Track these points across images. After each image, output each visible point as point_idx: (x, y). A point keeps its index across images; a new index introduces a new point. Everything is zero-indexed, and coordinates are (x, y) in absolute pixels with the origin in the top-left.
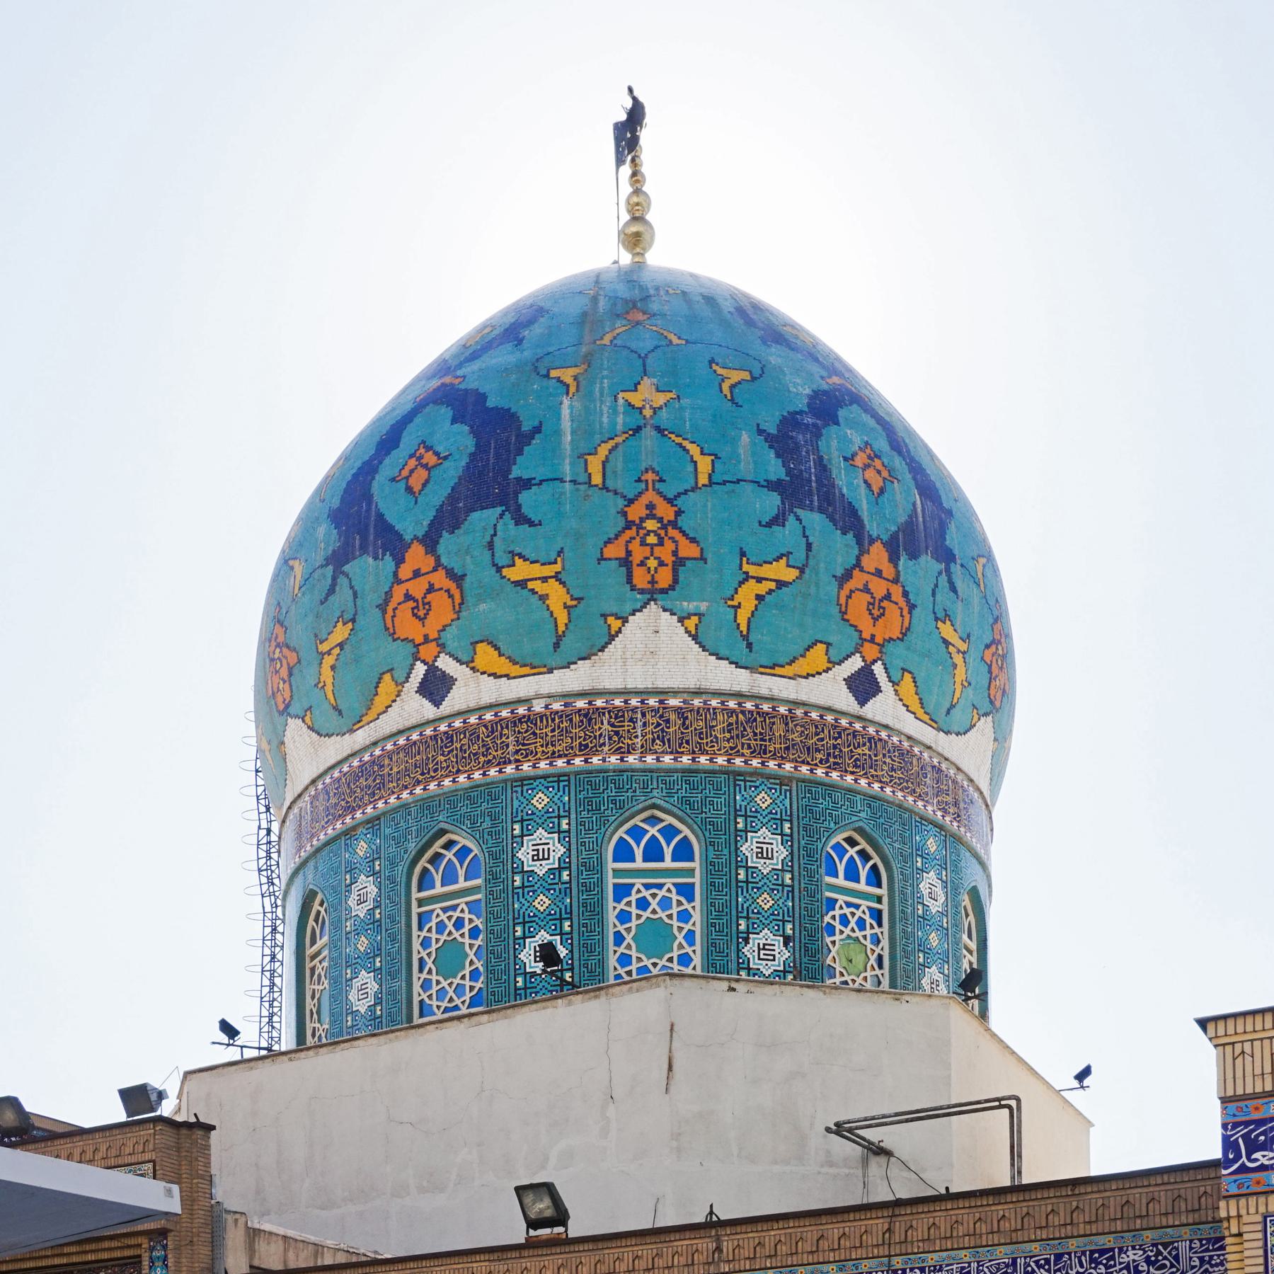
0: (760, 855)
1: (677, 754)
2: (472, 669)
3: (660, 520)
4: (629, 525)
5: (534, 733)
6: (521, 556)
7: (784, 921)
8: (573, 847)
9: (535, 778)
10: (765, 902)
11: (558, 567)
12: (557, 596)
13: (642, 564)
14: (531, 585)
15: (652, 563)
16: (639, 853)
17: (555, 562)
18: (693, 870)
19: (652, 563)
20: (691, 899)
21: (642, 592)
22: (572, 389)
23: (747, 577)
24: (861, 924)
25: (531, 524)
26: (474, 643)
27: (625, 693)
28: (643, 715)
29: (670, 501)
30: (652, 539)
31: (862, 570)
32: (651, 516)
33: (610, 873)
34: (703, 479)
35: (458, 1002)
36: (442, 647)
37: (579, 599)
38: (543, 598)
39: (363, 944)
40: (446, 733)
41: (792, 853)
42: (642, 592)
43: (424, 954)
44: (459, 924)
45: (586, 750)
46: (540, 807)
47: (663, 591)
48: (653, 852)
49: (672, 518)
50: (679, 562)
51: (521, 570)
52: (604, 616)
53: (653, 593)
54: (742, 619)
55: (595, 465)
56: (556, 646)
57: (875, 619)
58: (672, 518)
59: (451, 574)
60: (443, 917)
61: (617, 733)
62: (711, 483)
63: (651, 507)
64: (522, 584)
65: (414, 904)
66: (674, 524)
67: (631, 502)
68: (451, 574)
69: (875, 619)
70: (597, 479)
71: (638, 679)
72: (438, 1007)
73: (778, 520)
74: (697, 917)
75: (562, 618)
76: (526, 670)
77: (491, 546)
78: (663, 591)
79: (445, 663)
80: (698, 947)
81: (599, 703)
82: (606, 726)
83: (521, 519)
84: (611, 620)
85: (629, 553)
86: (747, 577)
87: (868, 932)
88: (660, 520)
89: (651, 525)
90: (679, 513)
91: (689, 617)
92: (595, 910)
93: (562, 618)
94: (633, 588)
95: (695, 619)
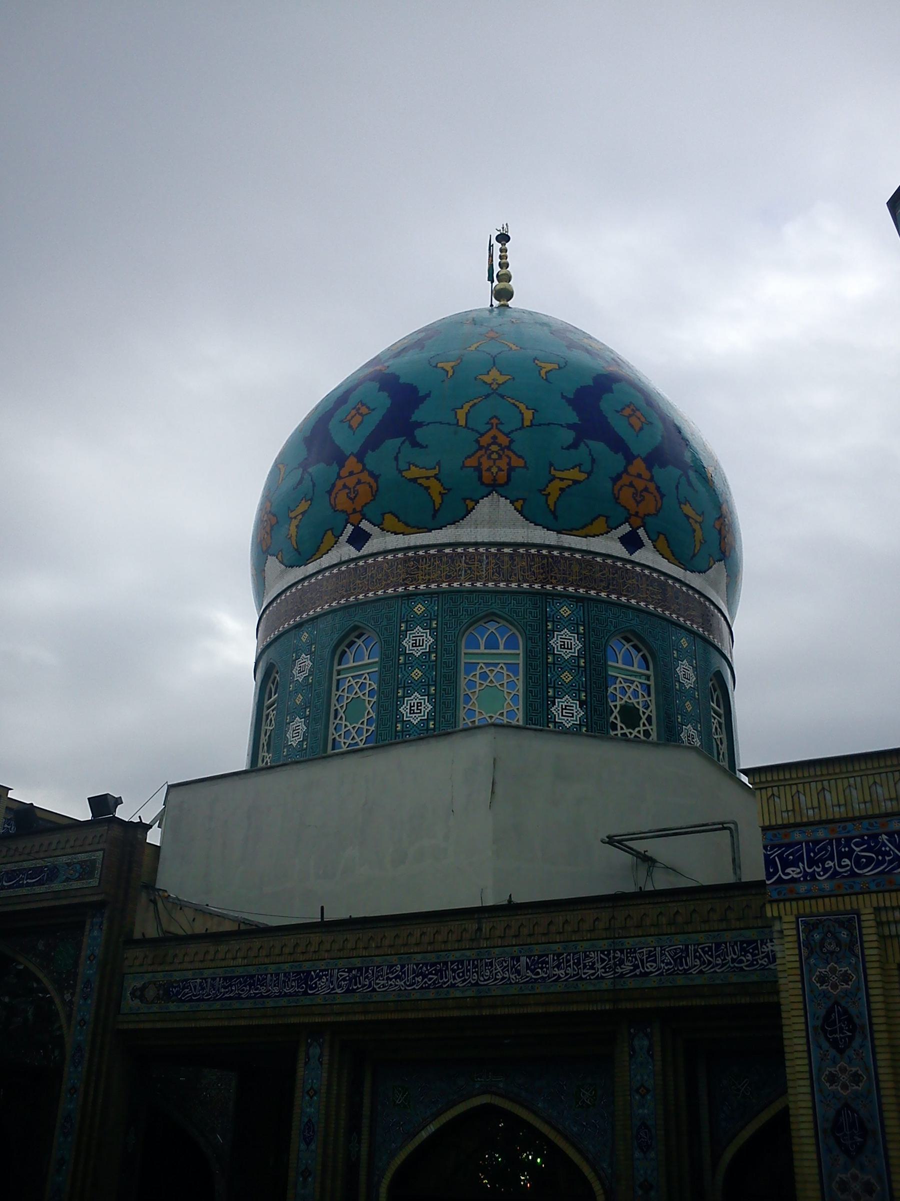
0: (563, 646)
1: (509, 582)
2: (383, 530)
3: (500, 445)
4: (481, 448)
5: (418, 568)
6: (414, 465)
7: (579, 690)
8: (439, 638)
9: (417, 595)
10: (567, 677)
11: (436, 471)
12: (436, 488)
13: (489, 469)
14: (419, 481)
15: (494, 470)
16: (482, 643)
17: (435, 468)
18: (519, 654)
19: (494, 470)
20: (516, 674)
21: (487, 485)
22: (450, 374)
23: (554, 478)
24: (635, 694)
25: (421, 446)
26: (383, 514)
27: (476, 545)
28: (487, 558)
29: (507, 435)
30: (495, 456)
31: (628, 474)
32: (494, 443)
33: (463, 654)
34: (527, 423)
35: (358, 740)
36: (364, 517)
37: (449, 490)
38: (427, 488)
39: (299, 699)
40: (362, 566)
41: (584, 646)
42: (487, 485)
43: (338, 707)
44: (362, 686)
45: (450, 579)
46: (419, 613)
47: (501, 485)
48: (492, 643)
49: (508, 444)
50: (511, 469)
51: (414, 472)
52: (465, 500)
53: (494, 487)
54: (551, 502)
55: (461, 414)
56: (434, 516)
57: (638, 503)
58: (508, 444)
59: (371, 474)
60: (353, 682)
61: (470, 568)
62: (532, 425)
63: (494, 438)
64: (414, 480)
65: (335, 673)
66: (508, 448)
67: (482, 435)
68: (371, 474)
69: (638, 503)
70: (462, 422)
71: (483, 534)
72: (345, 743)
73: (575, 445)
74: (520, 685)
75: (438, 500)
76: (415, 530)
77: (396, 458)
78: (501, 485)
79: (365, 525)
80: (521, 706)
81: (459, 550)
82: (463, 564)
83: (415, 444)
84: (468, 502)
85: (480, 464)
86: (554, 478)
87: (640, 699)
88: (500, 445)
89: (494, 448)
90: (512, 441)
91: (517, 500)
92: (452, 681)
93: (438, 500)
94: (482, 483)
95: (521, 502)
